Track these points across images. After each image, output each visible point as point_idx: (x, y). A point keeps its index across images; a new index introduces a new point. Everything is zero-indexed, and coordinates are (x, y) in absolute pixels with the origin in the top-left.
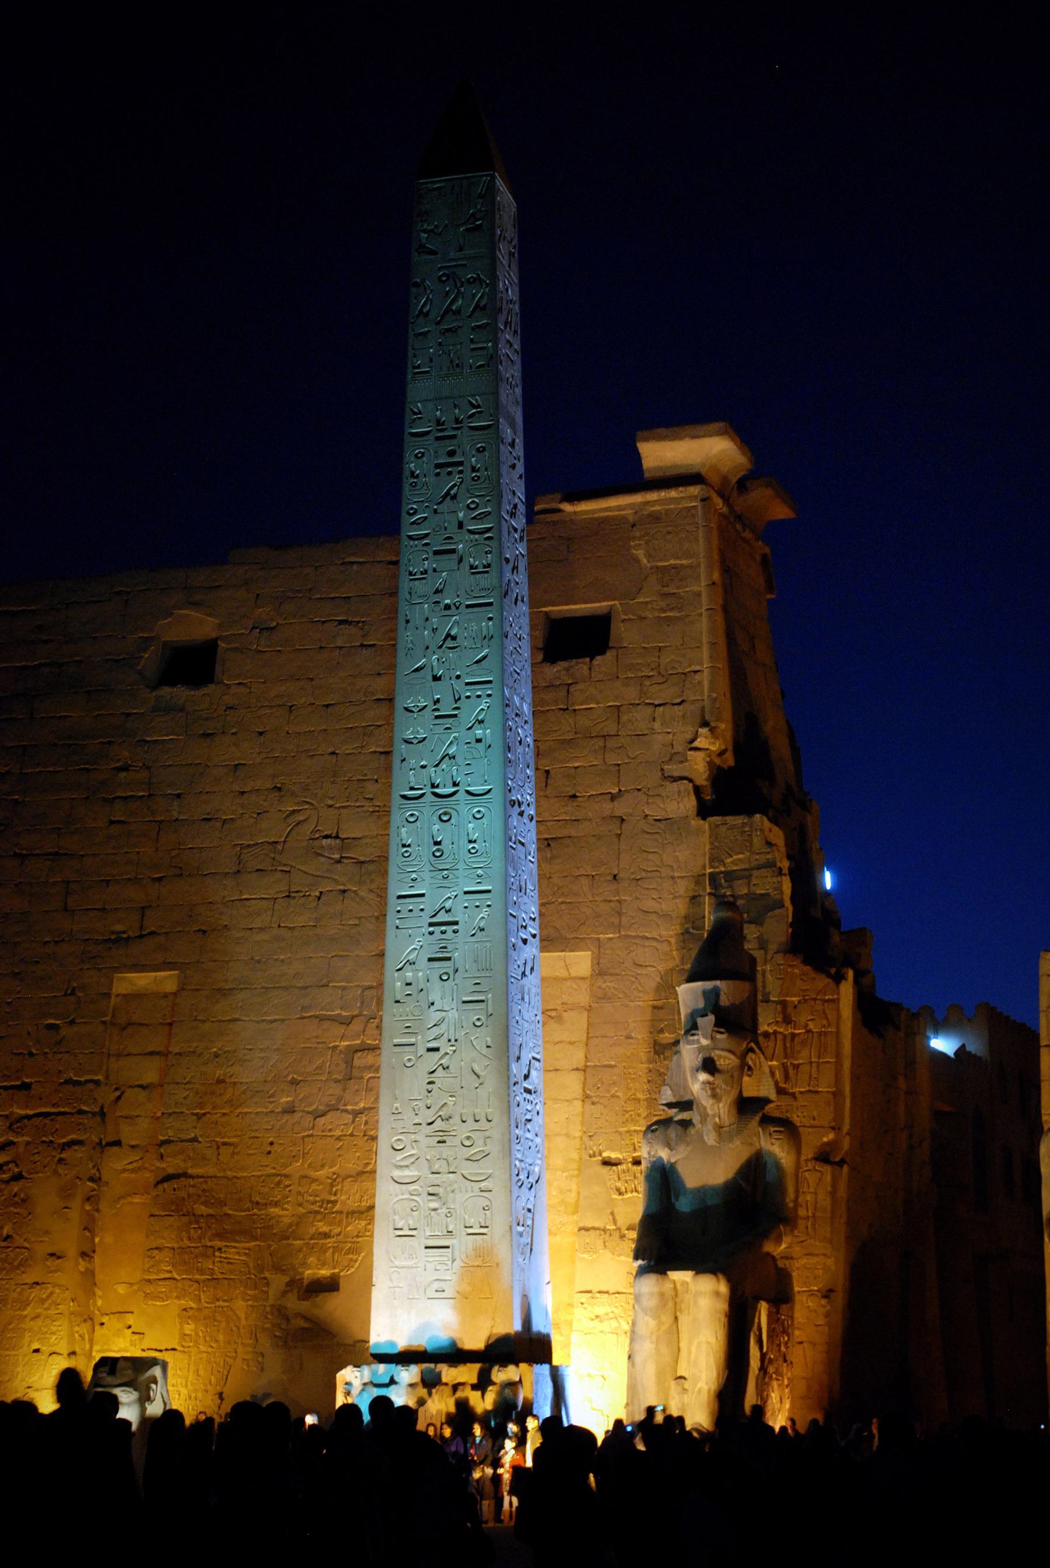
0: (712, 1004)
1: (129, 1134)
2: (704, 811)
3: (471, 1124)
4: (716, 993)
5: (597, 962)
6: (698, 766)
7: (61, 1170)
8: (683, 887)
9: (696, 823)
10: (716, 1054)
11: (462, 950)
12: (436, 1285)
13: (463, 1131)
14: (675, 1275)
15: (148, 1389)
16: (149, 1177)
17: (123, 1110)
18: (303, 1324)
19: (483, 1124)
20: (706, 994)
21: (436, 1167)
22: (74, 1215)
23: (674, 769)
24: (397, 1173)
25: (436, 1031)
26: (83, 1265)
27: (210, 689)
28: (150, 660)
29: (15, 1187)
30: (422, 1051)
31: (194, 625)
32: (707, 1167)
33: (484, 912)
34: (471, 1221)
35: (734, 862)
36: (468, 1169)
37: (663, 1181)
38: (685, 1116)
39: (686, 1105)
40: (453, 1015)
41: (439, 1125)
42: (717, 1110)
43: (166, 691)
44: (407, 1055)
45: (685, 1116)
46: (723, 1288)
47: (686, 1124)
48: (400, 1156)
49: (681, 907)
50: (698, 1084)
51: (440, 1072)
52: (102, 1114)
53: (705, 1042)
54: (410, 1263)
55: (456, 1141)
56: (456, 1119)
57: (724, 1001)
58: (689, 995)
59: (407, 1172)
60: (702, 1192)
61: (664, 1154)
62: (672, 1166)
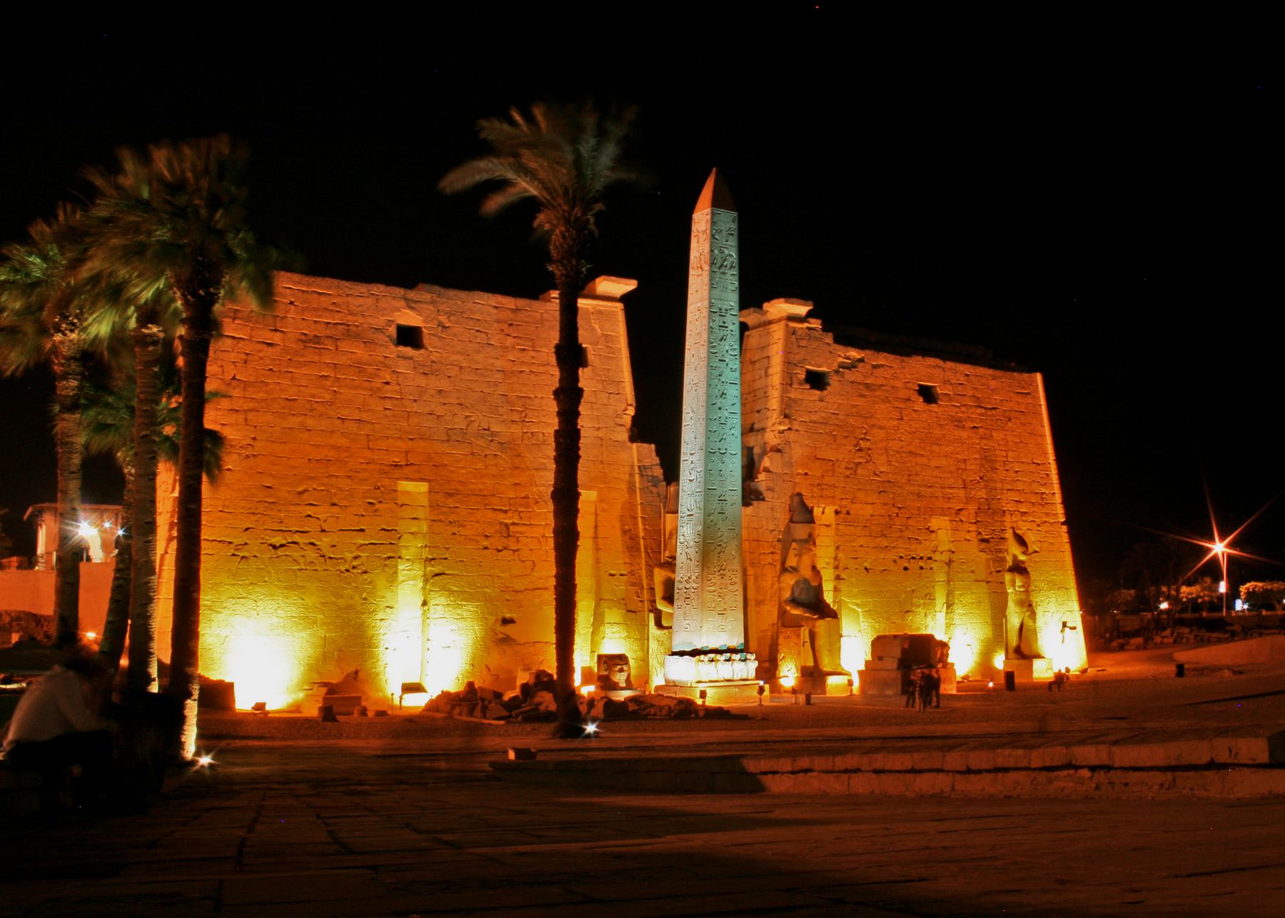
5: (599, 494)
23: (618, 420)
35: (647, 462)
49: (627, 477)
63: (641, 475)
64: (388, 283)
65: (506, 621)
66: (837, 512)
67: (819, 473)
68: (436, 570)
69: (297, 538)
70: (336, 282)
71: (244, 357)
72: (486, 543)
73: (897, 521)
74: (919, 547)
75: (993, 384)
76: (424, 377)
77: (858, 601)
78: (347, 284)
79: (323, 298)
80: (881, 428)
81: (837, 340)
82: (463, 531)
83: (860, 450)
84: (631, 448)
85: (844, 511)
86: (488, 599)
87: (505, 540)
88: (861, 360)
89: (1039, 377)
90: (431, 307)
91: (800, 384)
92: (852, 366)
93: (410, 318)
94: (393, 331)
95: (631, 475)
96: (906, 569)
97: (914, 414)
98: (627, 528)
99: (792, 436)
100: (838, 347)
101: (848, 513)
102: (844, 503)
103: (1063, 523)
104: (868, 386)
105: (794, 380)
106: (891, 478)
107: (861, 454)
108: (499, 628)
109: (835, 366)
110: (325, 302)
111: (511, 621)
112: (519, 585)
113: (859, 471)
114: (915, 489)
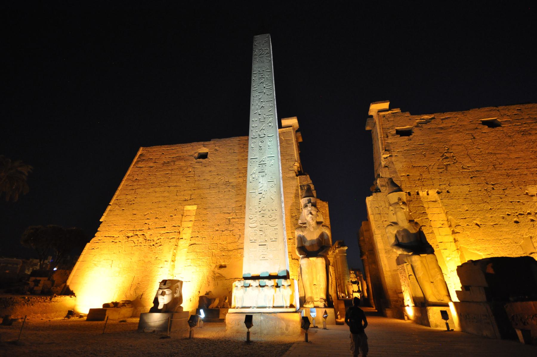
0: (309, 202)
1: (184, 236)
2: (297, 176)
3: (271, 212)
4: (310, 200)
6: (295, 168)
7: (170, 243)
8: (295, 188)
9: (296, 177)
10: (312, 211)
11: (267, 169)
12: (262, 256)
13: (269, 213)
14: (311, 259)
15: (176, 289)
16: (188, 245)
17: (184, 232)
18: (218, 275)
19: (275, 211)
20: (308, 200)
21: (262, 223)
22: (171, 253)
24: (251, 225)
25: (261, 189)
26: (172, 263)
27: (206, 159)
28: (196, 155)
29: (160, 247)
30: (257, 193)
31: (204, 150)
32: (312, 235)
33: (273, 161)
34: (272, 238)
35: (305, 183)
36: (271, 223)
37: (301, 239)
38: (304, 225)
39: (305, 223)
41: (262, 212)
42: (313, 223)
43: (198, 160)
44: (253, 195)
45: (304, 225)
46: (324, 262)
47: (305, 227)
48: (251, 220)
49: (295, 191)
50: (309, 218)
51: (262, 199)
52: (179, 232)
53: (309, 209)
54: (254, 250)
55: (267, 216)
56: (267, 210)
57: (312, 201)
58: (303, 201)
59: (253, 225)
60: (312, 241)
61: (301, 234)
62: (304, 236)
63: (302, 189)
65: (221, 267)
66: (438, 193)
68: (192, 242)
69: (138, 233)
74: (522, 206)
77: (478, 247)
80: (459, 145)
82: (208, 224)
83: (447, 158)
84: (297, 179)
85: (445, 191)
86: (213, 255)
87: (227, 226)
88: (433, 118)
91: (393, 135)
92: (427, 122)
95: (297, 190)
96: (517, 222)
97: (483, 134)
98: (294, 215)
99: (393, 159)
100: (414, 116)
101: (448, 192)
102: (442, 187)
104: (442, 128)
105: (389, 134)
106: (478, 168)
108: (217, 270)
109: (415, 124)
111: (225, 267)
112: (230, 247)
113: (449, 168)
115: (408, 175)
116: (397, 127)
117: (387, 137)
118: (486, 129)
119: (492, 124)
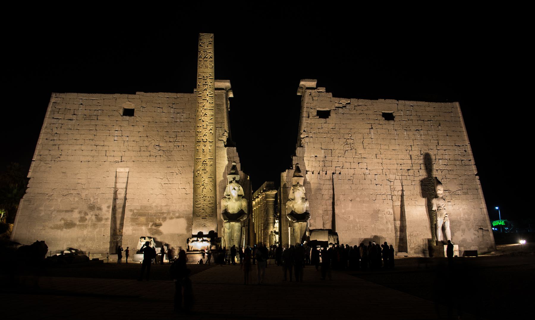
40: (207, 180)
64: (121, 93)
67: (323, 155)
70: (100, 95)
71: (60, 125)
72: (151, 192)
73: (369, 176)
75: (428, 109)
76: (133, 127)
78: (104, 95)
79: (94, 101)
81: (334, 96)
85: (338, 172)
89: (457, 104)
90: (139, 100)
93: (129, 106)
94: (121, 112)
100: (334, 98)
101: (340, 173)
103: (476, 175)
107: (347, 146)
110: (95, 102)
114: (380, 161)
115: (316, 156)
116: (319, 107)
117: (309, 117)
118: (382, 121)
119: (388, 117)
